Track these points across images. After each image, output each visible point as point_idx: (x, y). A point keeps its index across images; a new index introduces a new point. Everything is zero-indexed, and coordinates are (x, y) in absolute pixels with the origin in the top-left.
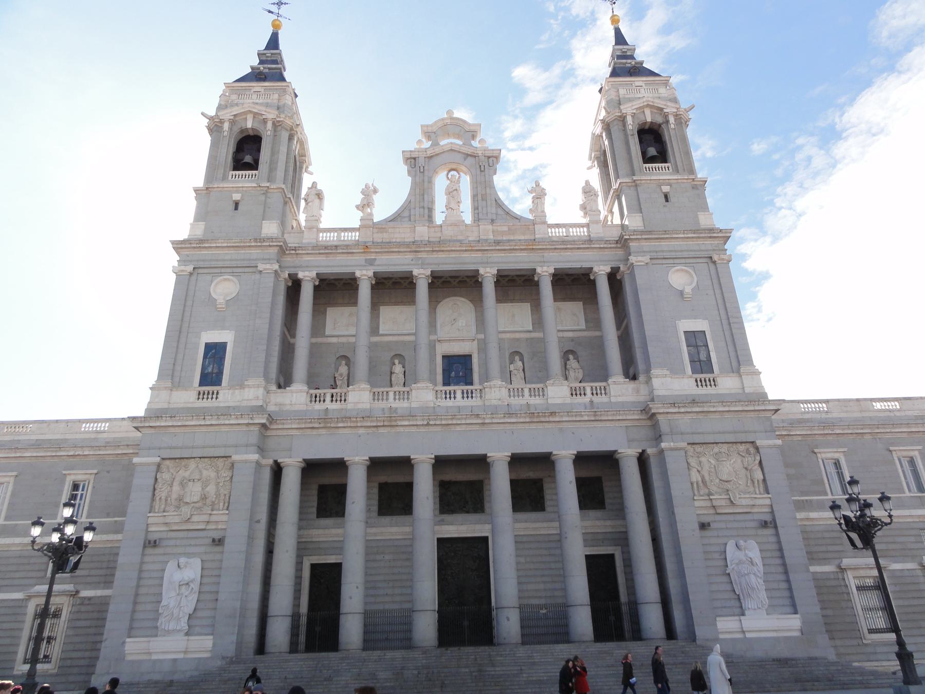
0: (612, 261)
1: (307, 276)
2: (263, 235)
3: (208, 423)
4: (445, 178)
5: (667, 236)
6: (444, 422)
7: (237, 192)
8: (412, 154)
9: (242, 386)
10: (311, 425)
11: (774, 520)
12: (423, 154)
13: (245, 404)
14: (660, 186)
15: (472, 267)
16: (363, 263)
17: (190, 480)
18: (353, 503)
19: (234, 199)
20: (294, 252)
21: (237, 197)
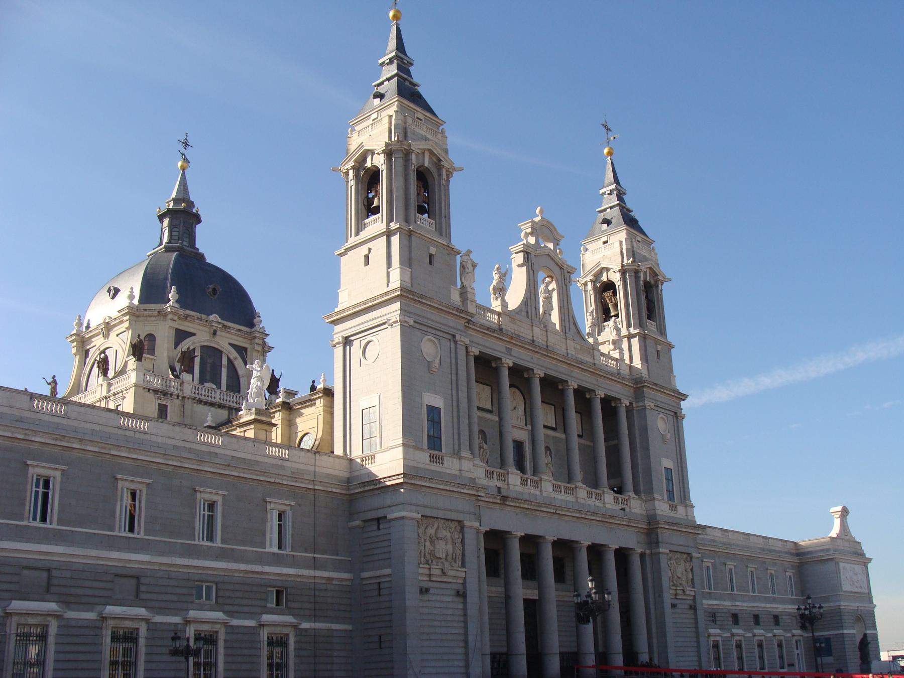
0: (630, 397)
1: (475, 351)
2: (452, 302)
3: (451, 489)
4: (542, 279)
5: (662, 390)
6: (564, 513)
7: (436, 246)
8: (528, 248)
9: (460, 458)
10: (494, 501)
11: (695, 606)
12: (534, 252)
13: (464, 474)
14: (656, 344)
15: (564, 377)
16: (505, 351)
17: (438, 538)
18: (518, 570)
19: (430, 252)
20: (467, 325)
21: (433, 250)
